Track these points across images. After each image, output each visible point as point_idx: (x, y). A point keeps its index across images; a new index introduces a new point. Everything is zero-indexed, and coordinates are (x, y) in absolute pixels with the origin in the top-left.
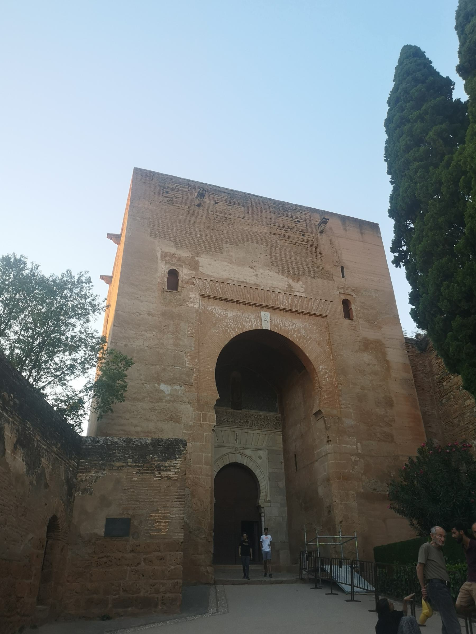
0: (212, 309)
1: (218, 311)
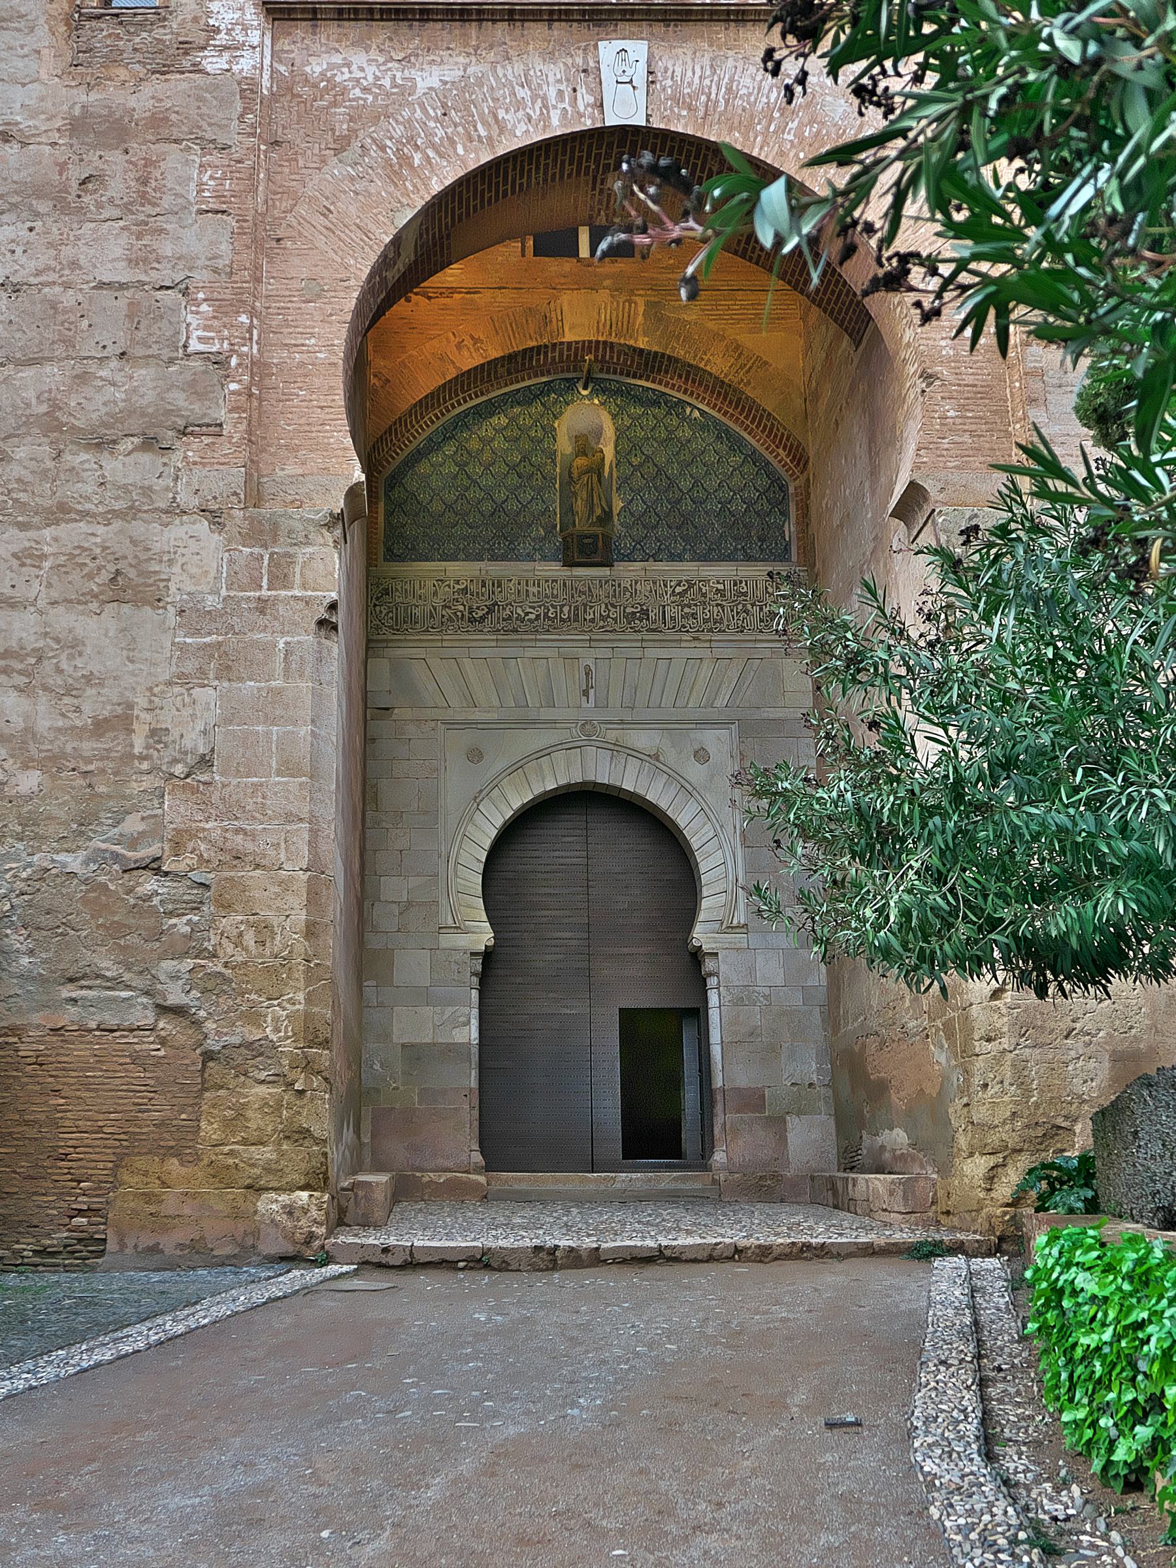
0: (331, 66)
1: (362, 75)
